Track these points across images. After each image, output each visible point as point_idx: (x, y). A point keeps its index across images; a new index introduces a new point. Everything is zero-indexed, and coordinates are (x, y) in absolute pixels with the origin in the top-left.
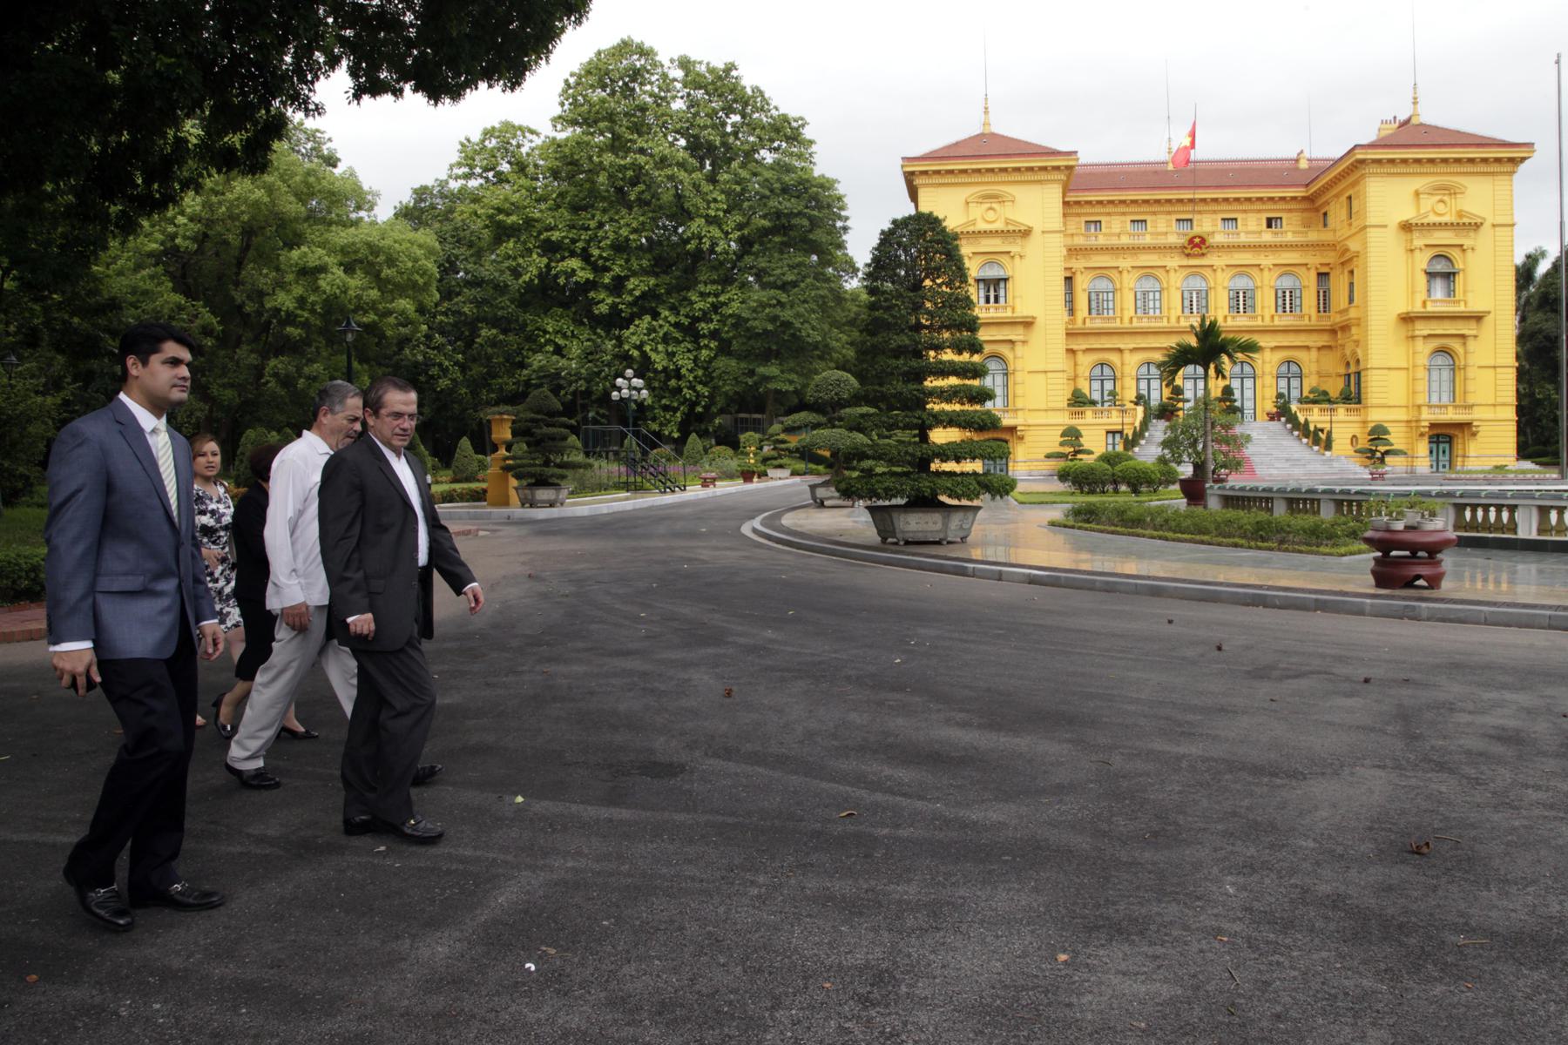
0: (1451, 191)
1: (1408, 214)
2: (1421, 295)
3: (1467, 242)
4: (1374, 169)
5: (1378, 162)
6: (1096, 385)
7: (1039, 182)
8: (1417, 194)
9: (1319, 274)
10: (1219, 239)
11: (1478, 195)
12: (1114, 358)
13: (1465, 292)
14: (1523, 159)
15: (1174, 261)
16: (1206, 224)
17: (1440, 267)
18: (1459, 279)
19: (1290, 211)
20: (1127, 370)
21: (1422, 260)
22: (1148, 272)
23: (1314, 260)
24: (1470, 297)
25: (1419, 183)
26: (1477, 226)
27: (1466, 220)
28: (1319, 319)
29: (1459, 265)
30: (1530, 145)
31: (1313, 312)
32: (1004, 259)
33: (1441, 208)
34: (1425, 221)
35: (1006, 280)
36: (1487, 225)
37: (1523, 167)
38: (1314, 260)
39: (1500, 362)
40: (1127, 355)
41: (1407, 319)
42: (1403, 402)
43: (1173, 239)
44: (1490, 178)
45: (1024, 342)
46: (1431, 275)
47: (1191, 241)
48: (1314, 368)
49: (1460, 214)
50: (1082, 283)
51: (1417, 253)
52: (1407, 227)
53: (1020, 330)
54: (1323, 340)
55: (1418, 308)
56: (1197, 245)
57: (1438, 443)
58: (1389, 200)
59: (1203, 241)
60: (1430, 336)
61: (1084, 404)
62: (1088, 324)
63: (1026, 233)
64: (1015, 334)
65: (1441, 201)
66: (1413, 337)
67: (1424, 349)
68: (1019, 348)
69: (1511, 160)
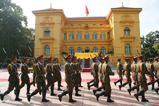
0: (128, 16)
3: (131, 25)
7: (56, 15)
9: (108, 32)
10: (91, 26)
11: (132, 17)
19: (104, 23)
20: (75, 48)
21: (123, 29)
22: (79, 32)
23: (107, 30)
28: (108, 40)
29: (130, 29)
30: (141, 9)
31: (107, 38)
32: (49, 28)
35: (50, 32)
37: (141, 13)
39: (138, 46)
41: (121, 38)
43: (83, 27)
45: (52, 43)
47: (86, 27)
48: (107, 48)
50: (68, 34)
53: (51, 40)
54: (109, 43)
59: (88, 27)
61: (64, 54)
63: (54, 23)
64: (51, 41)
68: (51, 44)
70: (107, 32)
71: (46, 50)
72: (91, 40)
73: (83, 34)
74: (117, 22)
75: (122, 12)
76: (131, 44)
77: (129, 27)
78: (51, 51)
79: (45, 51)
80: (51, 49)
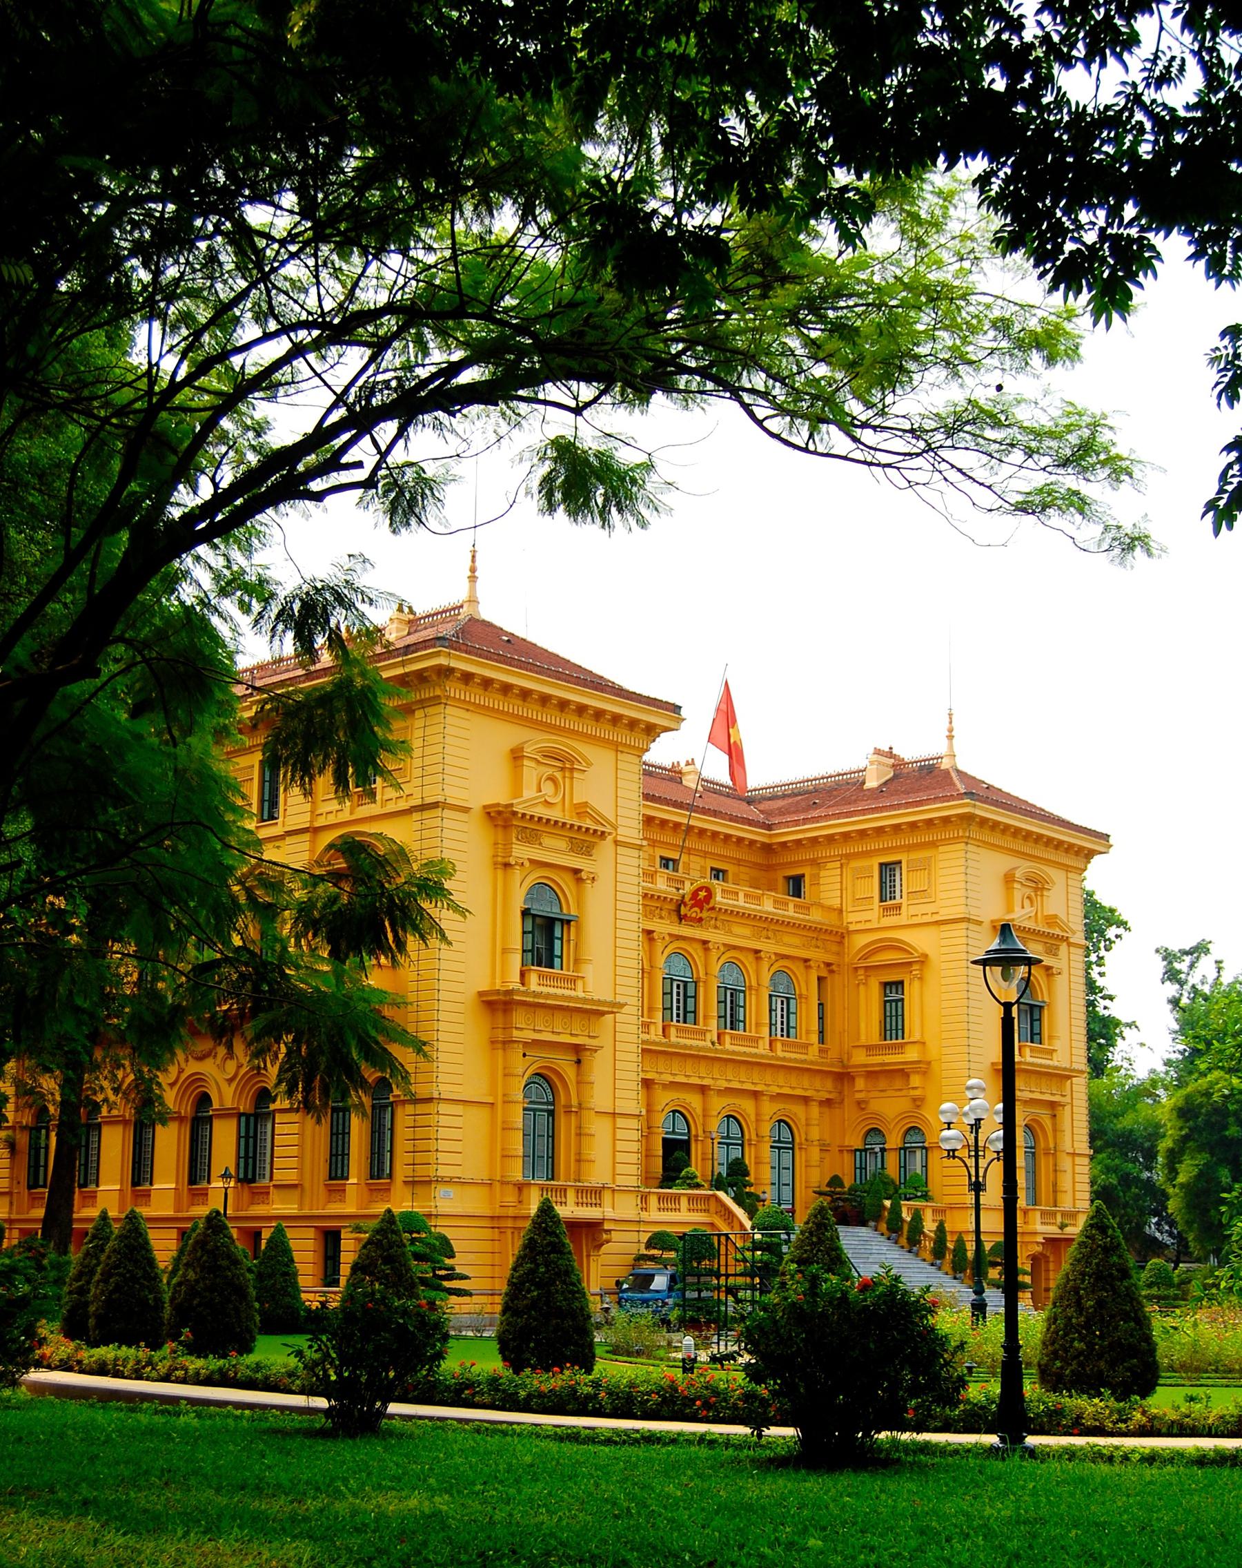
1: (499, 795)
2: (516, 960)
4: (454, 689)
5: (467, 677)
8: (517, 756)
13: (577, 961)
24: (588, 971)
27: (588, 823)
33: (548, 788)
36: (610, 838)
42: (483, 1175)
49: (582, 810)
51: (517, 874)
52: (501, 818)
55: (514, 981)
60: (536, 1043)
65: (552, 779)
66: (507, 1043)
67: (522, 1067)
74: (466, 810)
76: (569, 1072)
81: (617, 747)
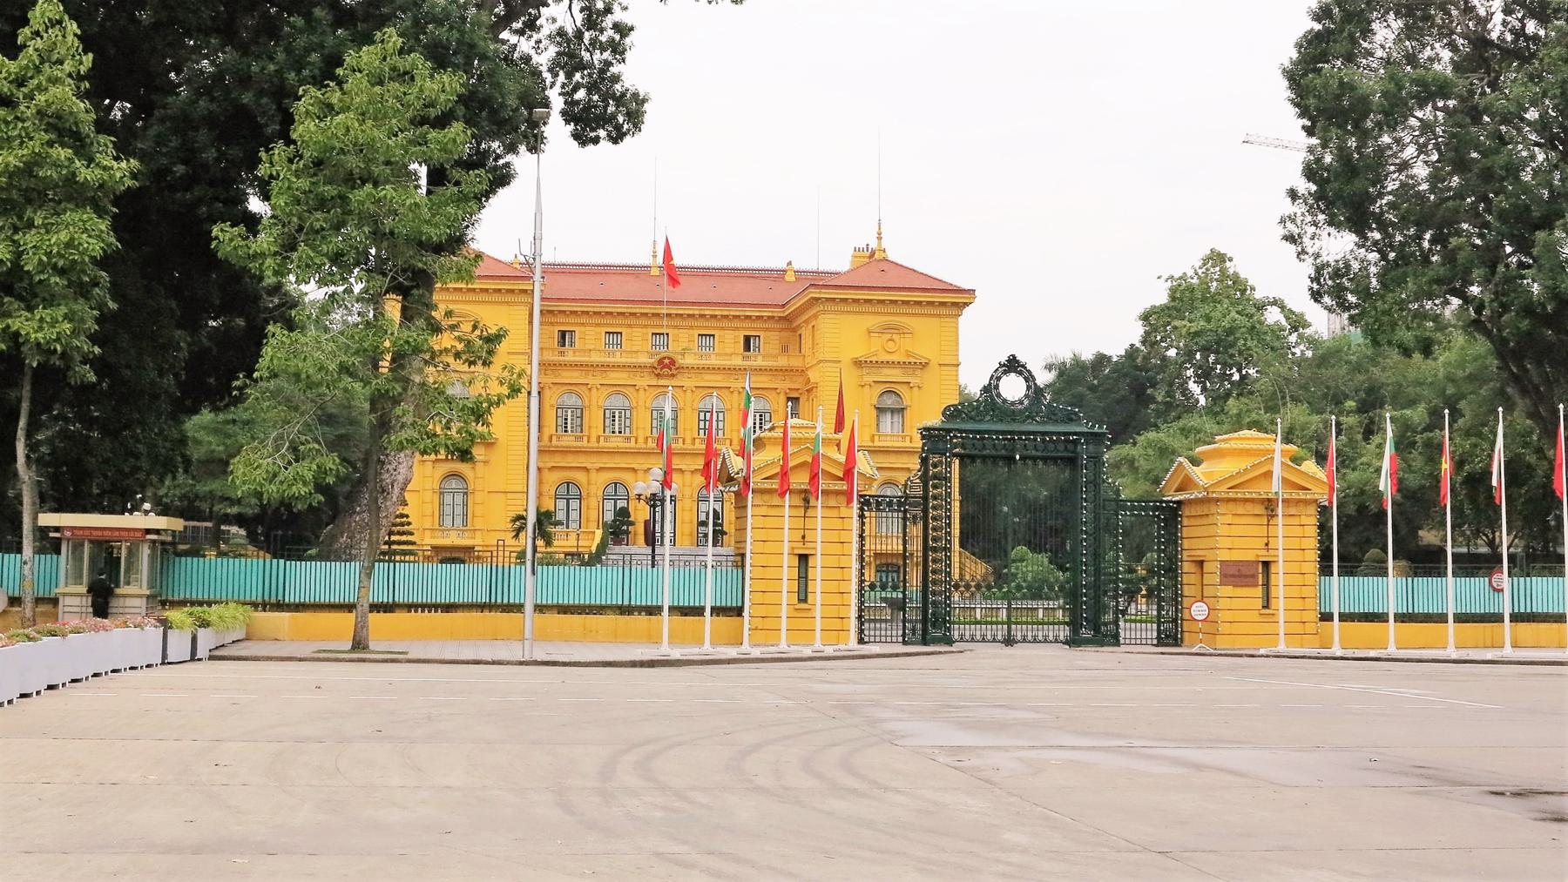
1: (860, 352)
4: (829, 306)
6: (562, 504)
10: (689, 360)
11: (923, 336)
12: (580, 477)
14: (966, 304)
15: (645, 380)
16: (682, 343)
17: (889, 402)
18: (908, 413)
19: (767, 329)
20: (593, 489)
23: (784, 385)
25: (873, 321)
26: (924, 366)
34: (874, 359)
37: (967, 311)
38: (784, 385)
40: (593, 475)
43: (644, 359)
44: (936, 320)
46: (880, 410)
47: (661, 361)
52: (858, 363)
56: (666, 367)
57: (887, 572)
58: (841, 338)
59: (673, 362)
62: (554, 442)
69: (955, 304)
70: (782, 398)
71: (448, 499)
72: (688, 441)
73: (641, 403)
75: (866, 308)
77: (900, 389)
78: (476, 509)
79: (442, 504)
80: (479, 497)
81: (939, 316)
